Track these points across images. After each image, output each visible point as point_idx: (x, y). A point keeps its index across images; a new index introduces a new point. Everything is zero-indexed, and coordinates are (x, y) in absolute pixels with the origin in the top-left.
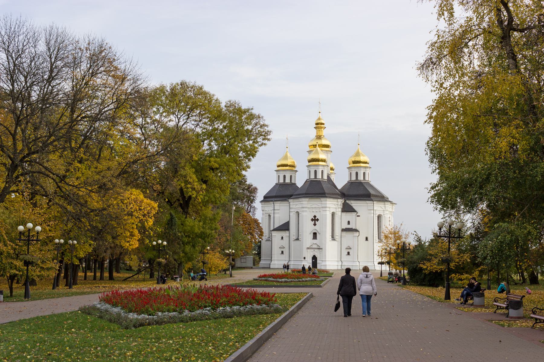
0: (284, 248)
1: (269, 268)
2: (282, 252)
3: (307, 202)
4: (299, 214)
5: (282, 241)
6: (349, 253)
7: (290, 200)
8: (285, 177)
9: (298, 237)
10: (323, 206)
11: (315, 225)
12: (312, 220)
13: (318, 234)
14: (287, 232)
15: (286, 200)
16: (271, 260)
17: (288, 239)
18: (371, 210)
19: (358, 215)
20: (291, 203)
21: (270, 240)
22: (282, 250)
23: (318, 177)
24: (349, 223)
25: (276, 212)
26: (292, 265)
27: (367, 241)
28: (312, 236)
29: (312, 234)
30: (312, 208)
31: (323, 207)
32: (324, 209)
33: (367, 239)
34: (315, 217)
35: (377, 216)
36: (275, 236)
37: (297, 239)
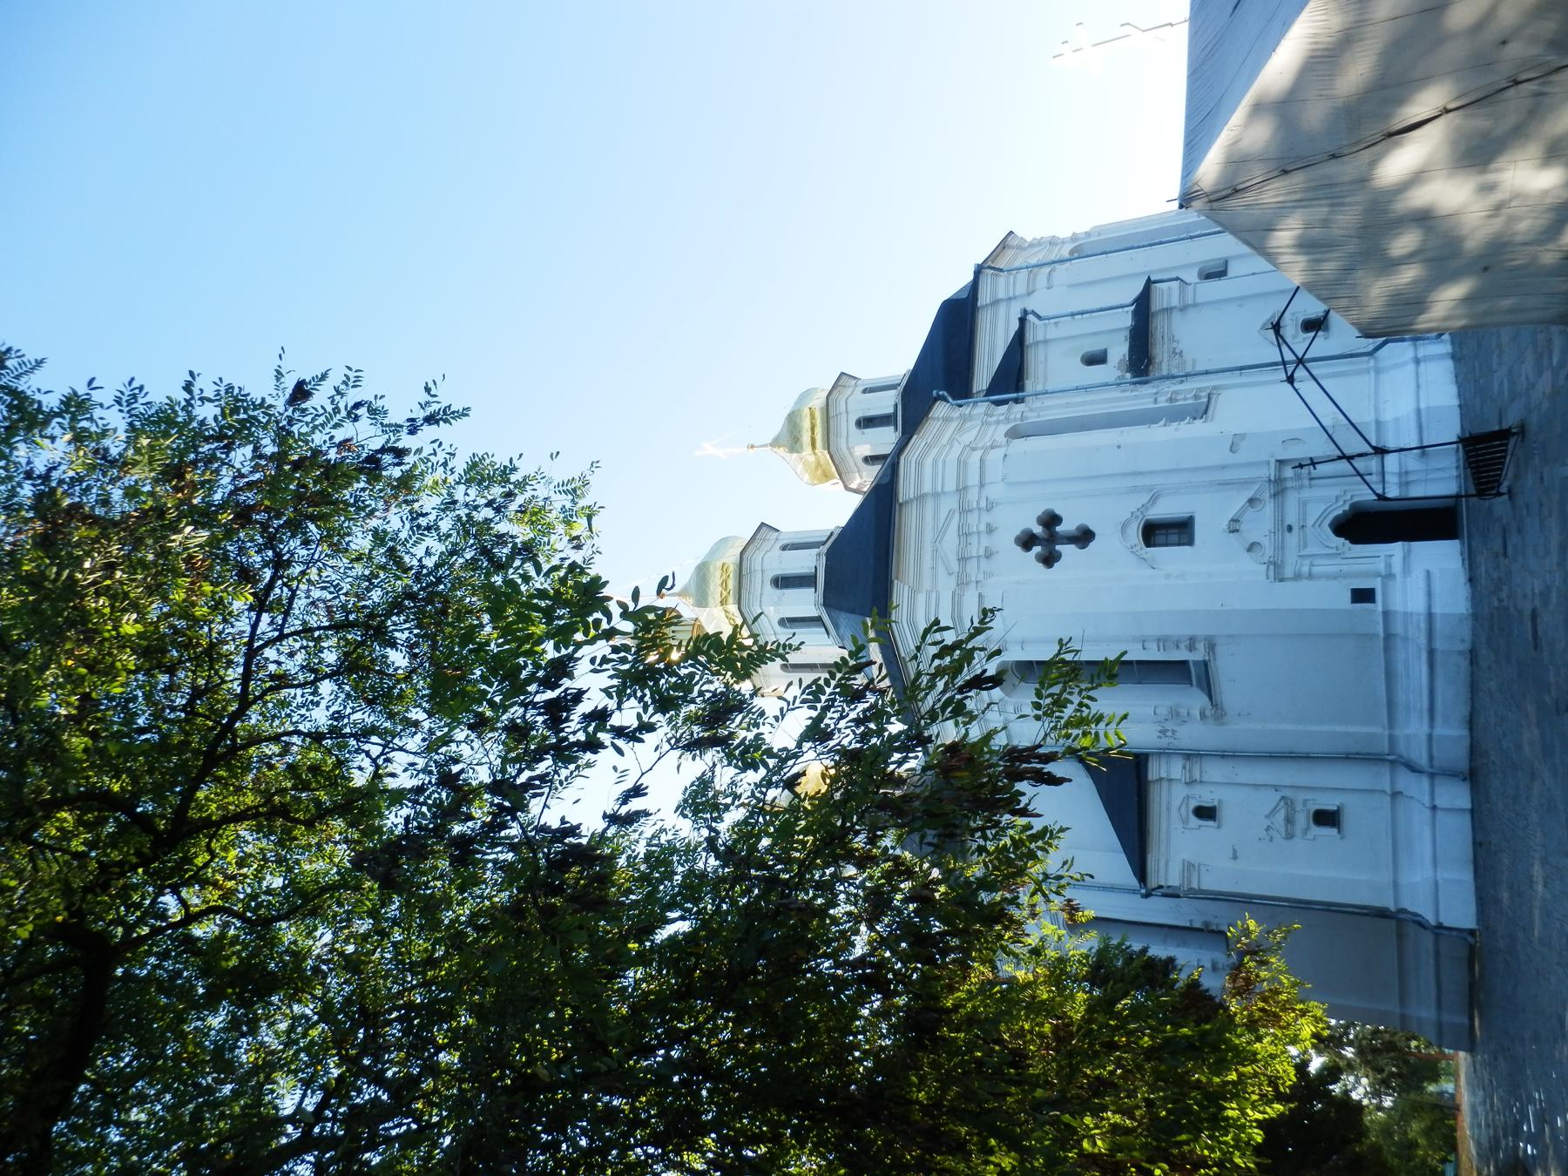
2: (1327, 818)
3: (921, 599)
5: (1225, 814)
10: (951, 486)
11: (1084, 537)
12: (1049, 560)
13: (1165, 510)
14: (1155, 770)
17: (1215, 771)
18: (1031, 281)
22: (1302, 819)
24: (1095, 359)
27: (1233, 270)
28: (1165, 555)
30: (963, 560)
31: (962, 490)
32: (973, 479)
34: (1027, 541)
36: (1189, 867)
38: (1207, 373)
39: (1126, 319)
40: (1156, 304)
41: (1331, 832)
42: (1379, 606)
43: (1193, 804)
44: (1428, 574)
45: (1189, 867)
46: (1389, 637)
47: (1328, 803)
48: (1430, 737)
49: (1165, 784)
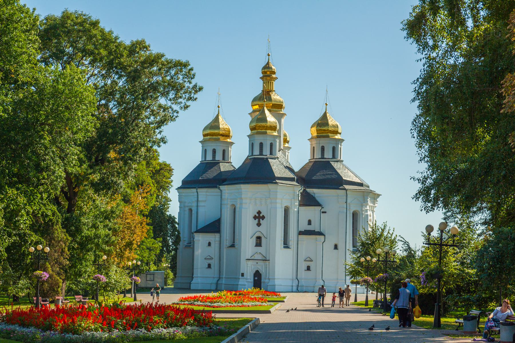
0: (212, 259)
1: (190, 289)
2: (209, 266)
4: (235, 209)
6: (308, 268)
7: (222, 187)
8: (214, 151)
9: (234, 242)
11: (259, 225)
12: (255, 218)
13: (263, 240)
14: (217, 235)
15: (216, 187)
16: (193, 278)
17: (217, 245)
19: (323, 210)
20: (223, 192)
21: (191, 245)
23: (264, 154)
24: (310, 222)
25: (200, 204)
26: (223, 285)
27: (336, 251)
28: (254, 241)
29: (254, 238)
33: (336, 247)
34: (259, 213)
35: (352, 212)
36: (199, 240)
37: (233, 246)
38: (298, 248)
39: (317, 230)
40: (318, 237)
41: (207, 266)
42: (241, 277)
43: (211, 242)
44: (245, 285)
45: (199, 240)
46: (236, 278)
47: (212, 266)
48: (222, 284)
49: (214, 236)
